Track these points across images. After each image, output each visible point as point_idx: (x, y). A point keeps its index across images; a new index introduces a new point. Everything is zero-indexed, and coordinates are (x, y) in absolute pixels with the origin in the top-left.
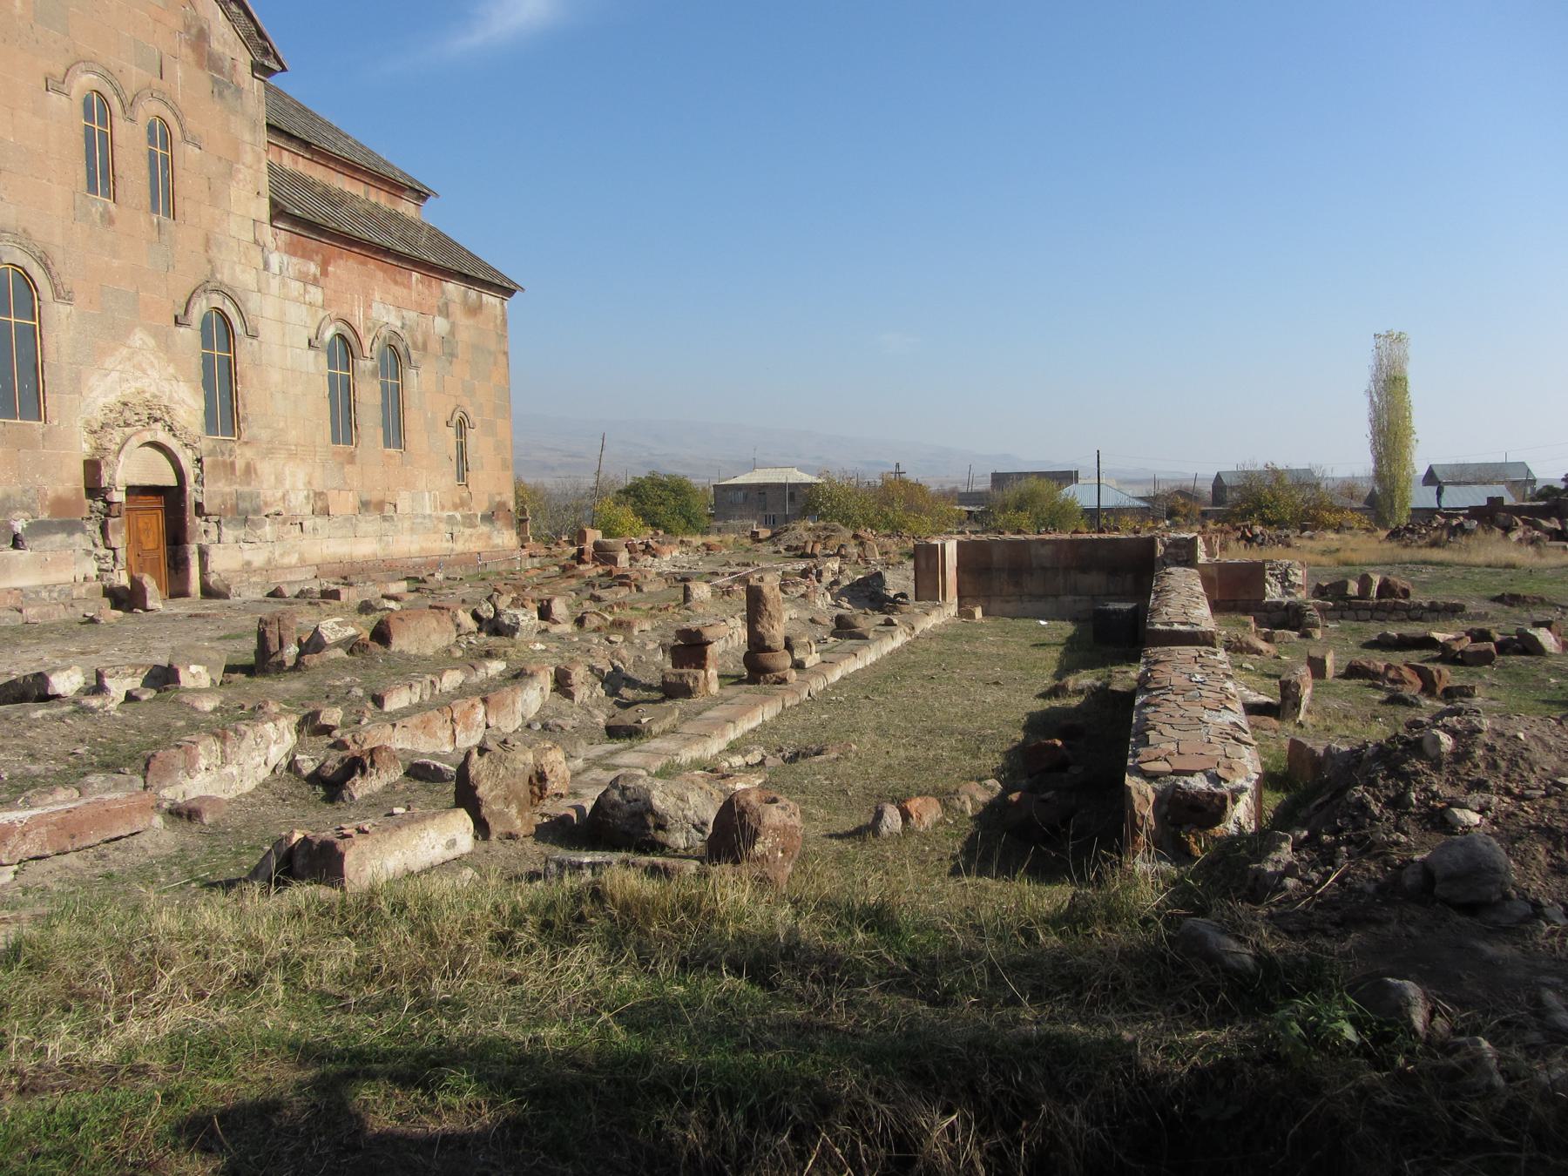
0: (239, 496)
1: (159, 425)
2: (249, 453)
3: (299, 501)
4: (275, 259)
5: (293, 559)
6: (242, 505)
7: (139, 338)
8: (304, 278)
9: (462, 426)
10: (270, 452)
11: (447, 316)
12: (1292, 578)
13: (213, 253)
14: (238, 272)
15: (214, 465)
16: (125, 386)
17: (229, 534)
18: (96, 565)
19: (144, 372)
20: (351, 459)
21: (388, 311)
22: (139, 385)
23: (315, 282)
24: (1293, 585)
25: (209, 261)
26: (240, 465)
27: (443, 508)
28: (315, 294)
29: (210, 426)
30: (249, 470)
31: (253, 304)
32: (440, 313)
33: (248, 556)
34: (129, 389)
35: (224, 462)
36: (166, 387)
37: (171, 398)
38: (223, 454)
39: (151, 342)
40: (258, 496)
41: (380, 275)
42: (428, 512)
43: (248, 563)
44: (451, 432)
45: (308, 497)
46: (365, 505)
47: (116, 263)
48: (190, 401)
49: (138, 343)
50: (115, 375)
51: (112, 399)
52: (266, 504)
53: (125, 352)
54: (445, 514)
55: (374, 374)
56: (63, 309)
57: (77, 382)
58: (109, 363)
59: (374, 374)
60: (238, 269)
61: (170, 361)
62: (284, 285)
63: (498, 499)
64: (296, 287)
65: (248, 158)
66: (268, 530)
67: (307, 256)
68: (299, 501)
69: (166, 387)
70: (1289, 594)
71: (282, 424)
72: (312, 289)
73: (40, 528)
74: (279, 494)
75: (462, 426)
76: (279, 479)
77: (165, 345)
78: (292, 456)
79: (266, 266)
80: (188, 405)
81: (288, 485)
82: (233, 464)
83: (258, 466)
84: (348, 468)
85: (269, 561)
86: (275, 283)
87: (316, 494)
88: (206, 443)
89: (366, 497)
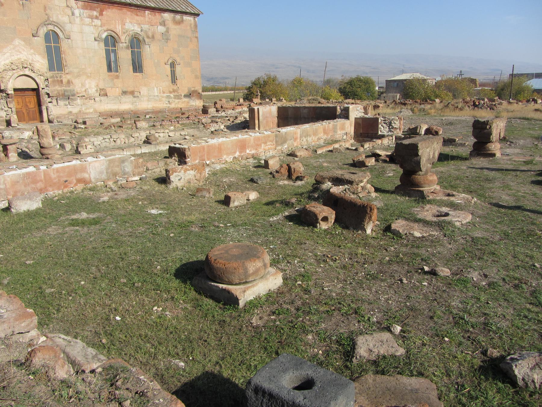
0: (65, 91)
1: (27, 69)
2: (69, 77)
3: (92, 91)
4: (77, 12)
5: (91, 110)
6: (66, 94)
7: (17, 42)
8: (91, 17)
9: (173, 65)
10: (78, 76)
11: (165, 25)
12: (393, 125)
13: (48, 12)
14: (60, 16)
15: (54, 81)
16: (12, 57)
17: (61, 103)
18: (5, 113)
19: (20, 52)
20: (117, 77)
21: (134, 26)
22: (18, 57)
23: (97, 18)
24: (393, 128)
25: (46, 15)
26: (65, 81)
27: (164, 93)
28: (98, 22)
29: (51, 68)
31: (68, 27)
32: (161, 24)
33: (70, 110)
34: (15, 58)
35: (58, 81)
36: (31, 57)
37: (32, 60)
38: (57, 77)
39: (23, 43)
40: (74, 90)
41: (129, 13)
42: (156, 94)
43: (71, 112)
44: (168, 67)
45: (97, 91)
46: (124, 93)
47: (5, 18)
48: (42, 61)
49: (17, 44)
50: (8, 54)
51: (7, 62)
52: (78, 93)
53: (12, 46)
54: (165, 95)
55: (127, 48)
58: (5, 50)
59: (127, 48)
60: (60, 16)
61: (31, 49)
62: (82, 20)
63: (193, 89)
64: (88, 20)
66: (79, 101)
67: (92, 9)
68: (92, 91)
69: (31, 57)
70: (390, 131)
71: (83, 67)
72: (96, 21)
74: (84, 90)
75: (173, 65)
76: (83, 85)
78: (88, 77)
79: (73, 14)
80: (41, 63)
81: (87, 87)
82: (62, 81)
83: (73, 81)
84: (115, 80)
85: (80, 111)
86: (78, 20)
87: (100, 89)
88: (49, 74)
89: (125, 90)
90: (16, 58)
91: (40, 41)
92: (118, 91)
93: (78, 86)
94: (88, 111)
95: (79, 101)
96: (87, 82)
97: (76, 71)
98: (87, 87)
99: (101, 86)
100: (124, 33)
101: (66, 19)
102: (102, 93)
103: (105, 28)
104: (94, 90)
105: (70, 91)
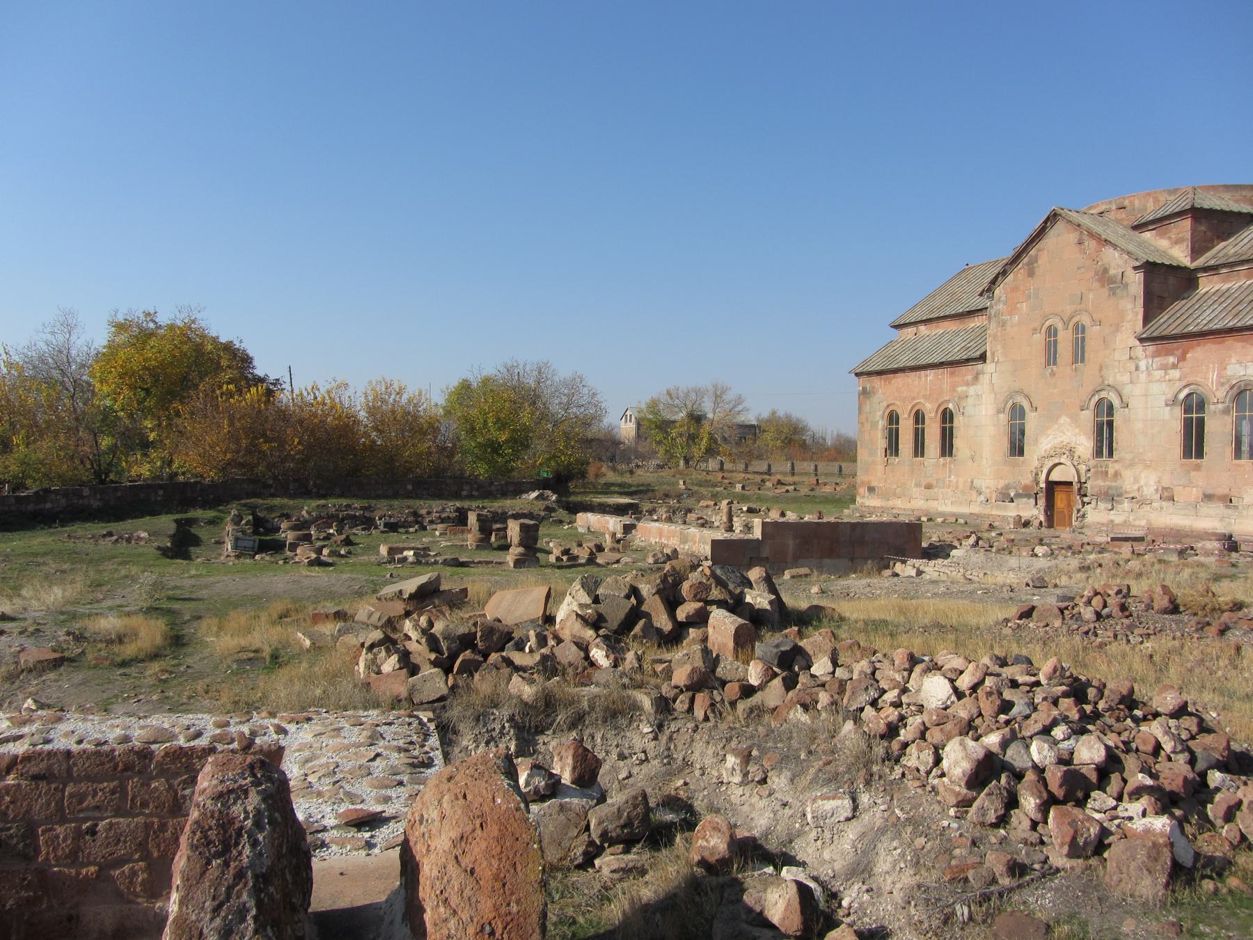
0: (1110, 487)
2: (1117, 466)
3: (1150, 491)
4: (1143, 364)
6: (1110, 492)
7: (1064, 420)
8: (1164, 368)
10: (1132, 464)
14: (1118, 376)
15: (1096, 473)
17: (1102, 505)
20: (1198, 468)
23: (1174, 366)
26: (1111, 471)
28: (1175, 374)
29: (1099, 453)
30: (1117, 475)
31: (1126, 391)
34: (1057, 441)
36: (1074, 439)
41: (1240, 344)
45: (1157, 490)
46: (1208, 497)
56: (1033, 414)
57: (1036, 441)
59: (1226, 411)
60: (1118, 376)
62: (1149, 374)
64: (1159, 374)
65: (1130, 316)
66: (1126, 505)
67: (1168, 353)
68: (1150, 491)
69: (1074, 439)
73: (1018, 495)
74: (1136, 487)
76: (1136, 480)
77: (1074, 419)
78: (1147, 467)
79: (1137, 368)
80: (1085, 445)
81: (1142, 483)
82: (1107, 473)
84: (1193, 474)
86: (1143, 377)
88: (1092, 463)
89: (1209, 491)
90: (1059, 440)
91: (1088, 416)
92: (1195, 493)
93: (1128, 482)
94: (1137, 523)
95: (1126, 505)
96: (1143, 475)
97: (1129, 456)
98: (1142, 483)
99: (1165, 483)
100: (1222, 384)
101: (1126, 378)
102: (1166, 494)
103: (1184, 383)
104: (1152, 489)
105: (1116, 488)
